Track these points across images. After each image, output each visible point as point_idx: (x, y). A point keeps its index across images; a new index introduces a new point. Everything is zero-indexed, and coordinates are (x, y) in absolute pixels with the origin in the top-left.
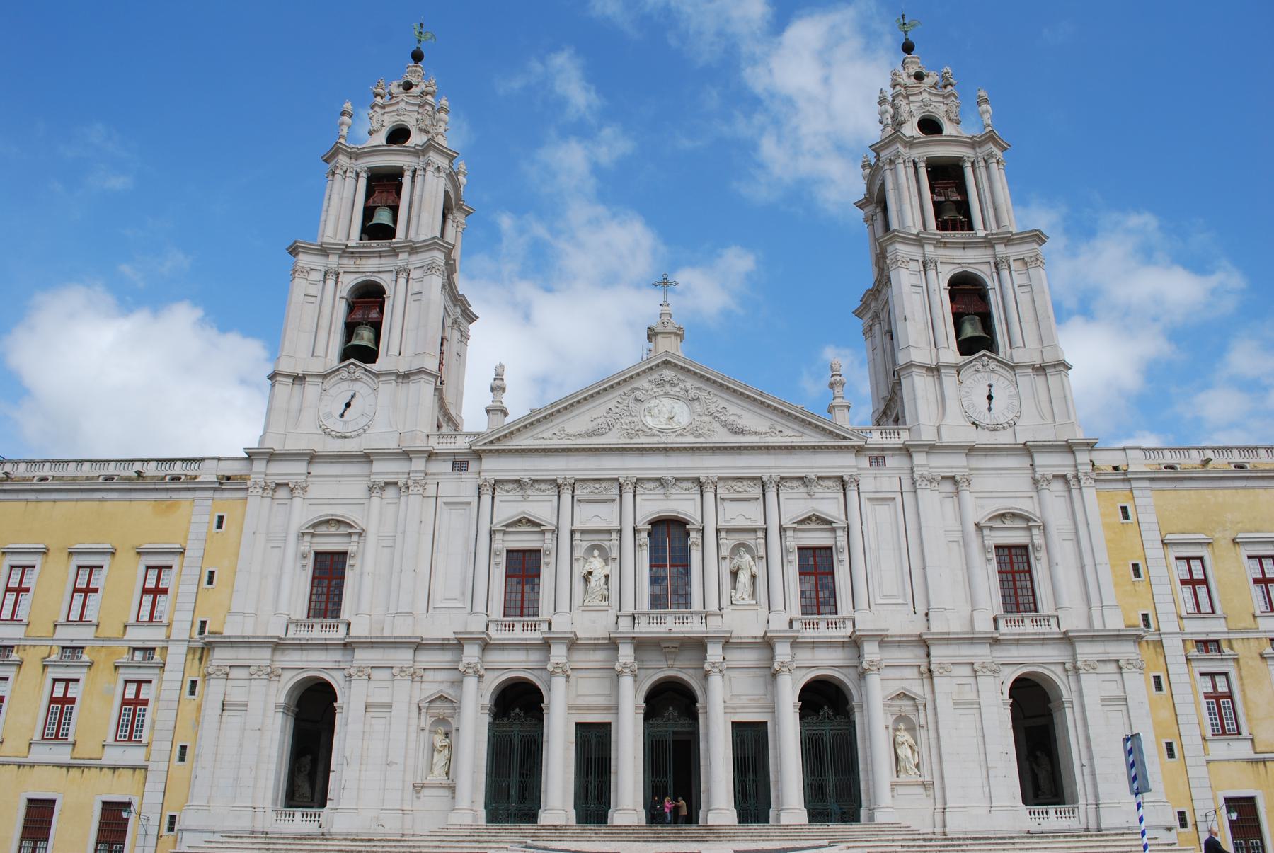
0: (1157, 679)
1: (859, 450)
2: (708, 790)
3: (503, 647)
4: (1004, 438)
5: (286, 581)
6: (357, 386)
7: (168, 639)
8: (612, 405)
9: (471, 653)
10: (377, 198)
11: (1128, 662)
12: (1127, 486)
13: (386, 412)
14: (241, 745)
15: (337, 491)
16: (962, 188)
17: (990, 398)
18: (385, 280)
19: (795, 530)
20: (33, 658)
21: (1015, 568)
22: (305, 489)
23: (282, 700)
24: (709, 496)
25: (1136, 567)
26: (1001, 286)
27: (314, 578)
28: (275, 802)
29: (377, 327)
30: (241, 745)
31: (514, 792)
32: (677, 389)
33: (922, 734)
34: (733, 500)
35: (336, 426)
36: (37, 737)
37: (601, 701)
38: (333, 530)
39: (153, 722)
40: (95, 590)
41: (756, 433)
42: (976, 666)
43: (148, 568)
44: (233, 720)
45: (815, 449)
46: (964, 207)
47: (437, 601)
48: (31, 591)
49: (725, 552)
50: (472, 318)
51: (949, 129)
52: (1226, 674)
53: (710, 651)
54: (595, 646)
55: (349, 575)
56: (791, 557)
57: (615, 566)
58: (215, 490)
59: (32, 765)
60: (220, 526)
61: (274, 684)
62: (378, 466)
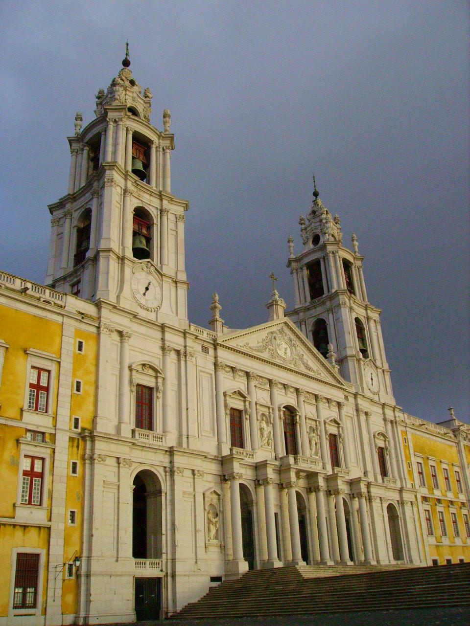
17: (372, 379)
18: (154, 212)
35: (142, 301)
57: (272, 427)
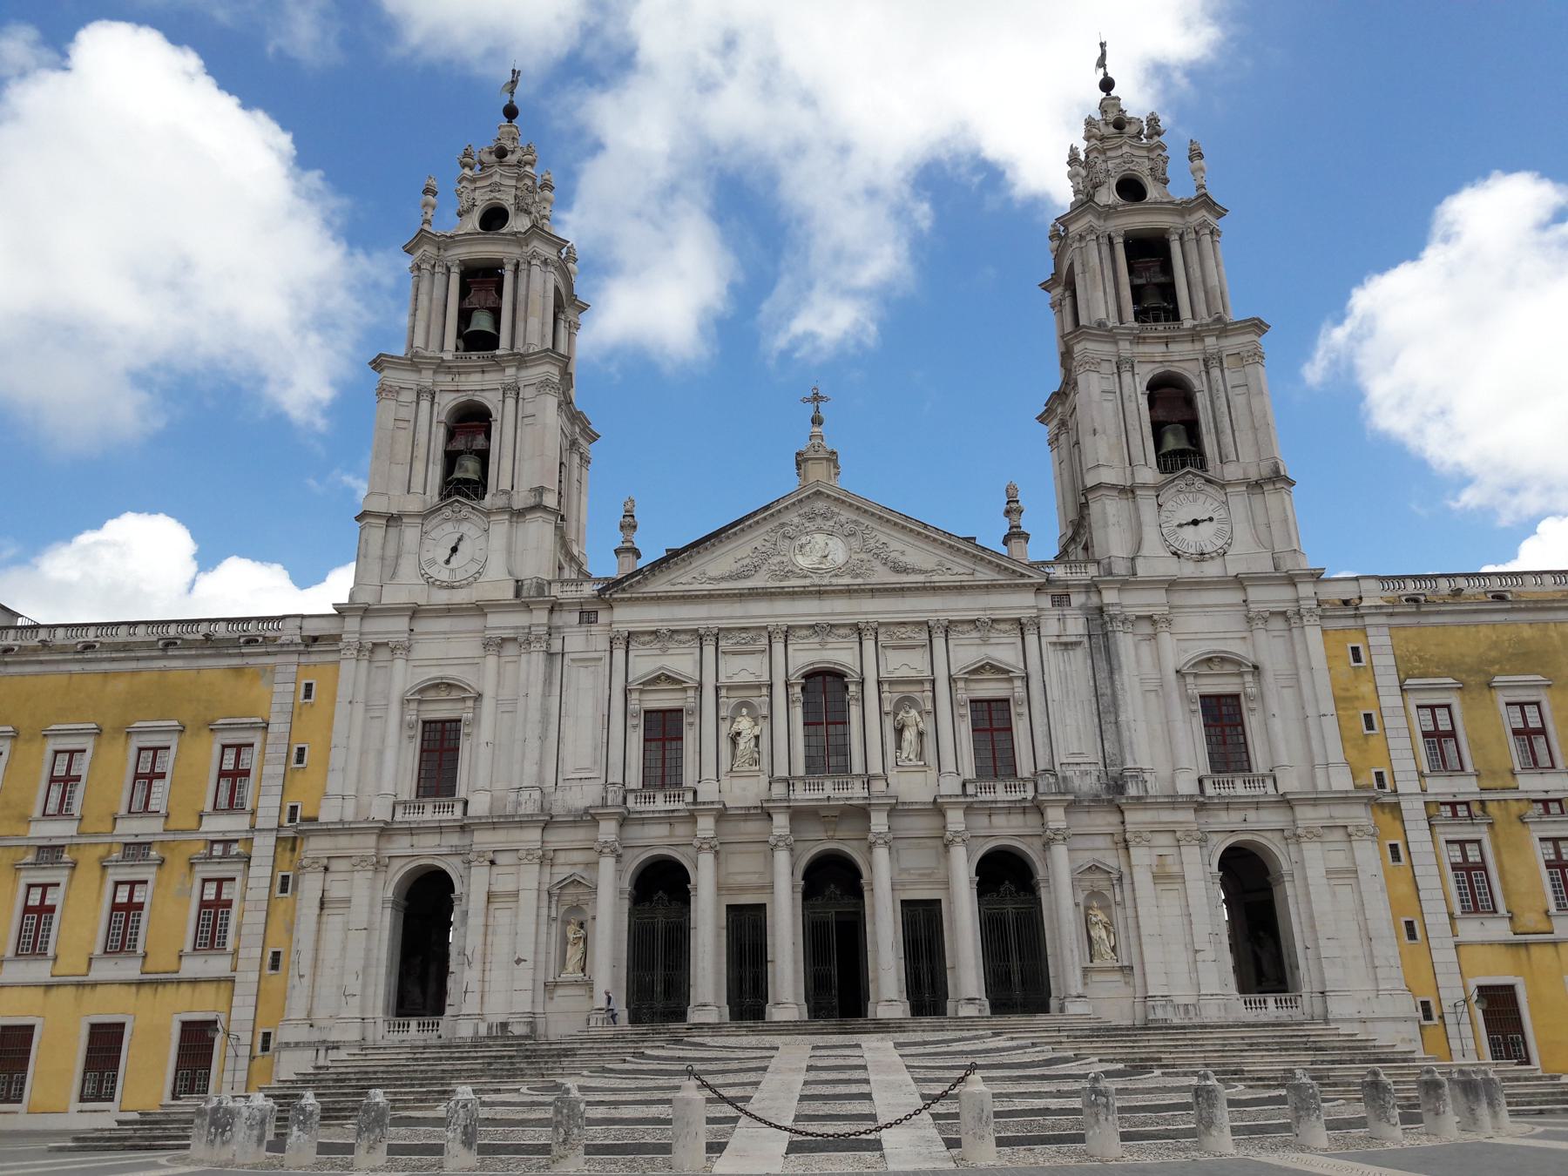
0: (1394, 847)
1: (1039, 589)
2: (877, 979)
3: (643, 821)
4: (1211, 569)
5: (390, 755)
6: (464, 527)
7: (252, 827)
8: (758, 543)
9: (608, 830)
10: (474, 299)
12: (1359, 622)
13: (496, 554)
14: (344, 949)
15: (446, 651)
16: (1167, 268)
18: (491, 401)
19: (966, 680)
20: (89, 858)
21: (1223, 720)
22: (408, 649)
23: (390, 894)
24: (869, 645)
25: (1368, 717)
26: (1210, 388)
27: (422, 751)
28: (386, 1012)
29: (483, 457)
30: (344, 949)
31: (659, 988)
32: (831, 523)
33: (1118, 914)
34: (894, 648)
35: (444, 575)
36: (98, 951)
37: (754, 879)
38: (443, 695)
39: (239, 926)
40: (162, 776)
41: (921, 572)
43: (224, 747)
44: (334, 921)
45: (989, 588)
46: (1168, 291)
47: (568, 770)
48: (83, 780)
49: (887, 708)
50: (593, 437)
51: (1153, 192)
52: (1478, 842)
53: (873, 821)
54: (747, 814)
55: (465, 747)
56: (963, 711)
57: (765, 725)
58: (300, 653)
59: (94, 985)
60: (308, 695)
61: (382, 876)
62: (494, 620)
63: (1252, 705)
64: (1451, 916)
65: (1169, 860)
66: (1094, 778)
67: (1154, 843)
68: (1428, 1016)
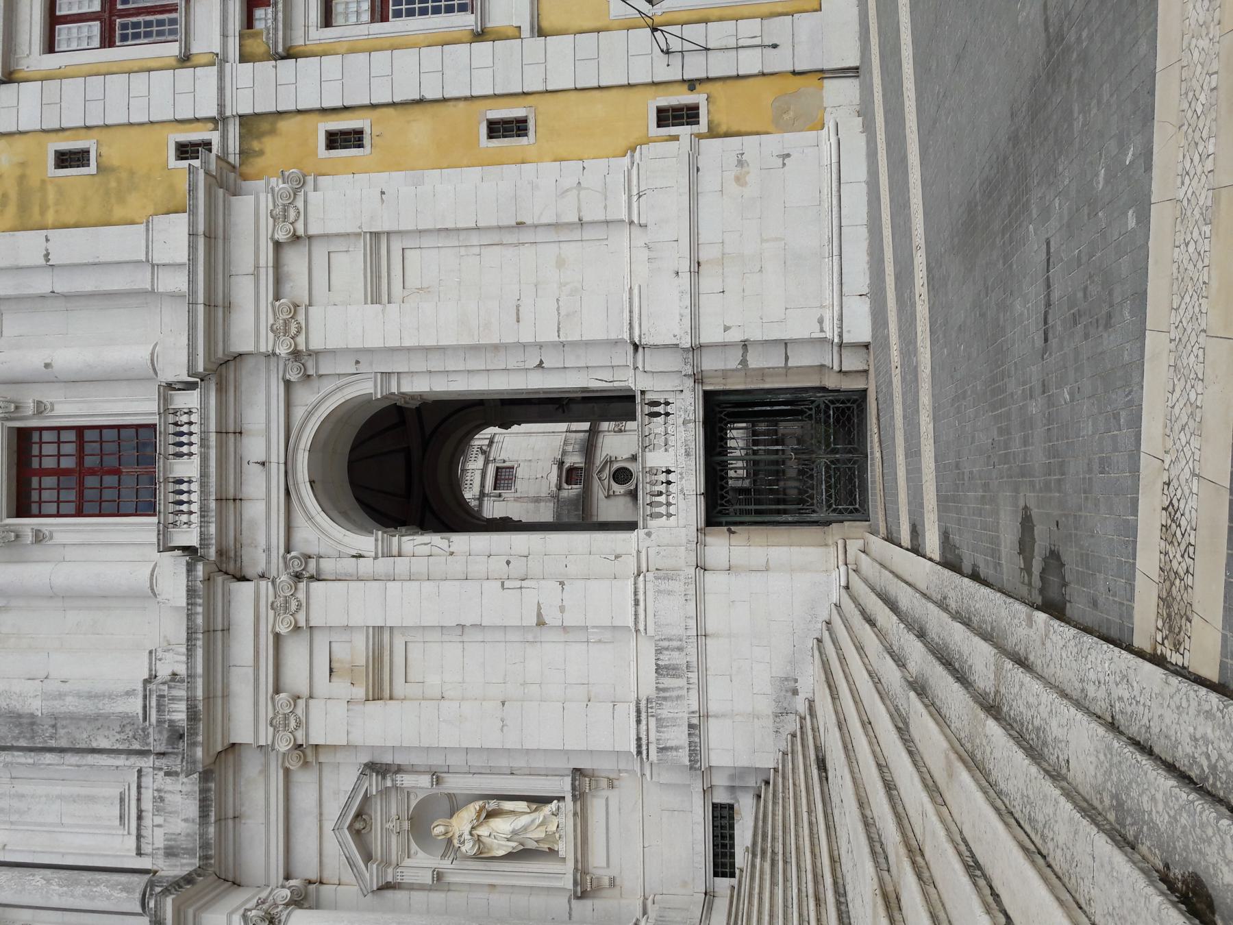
0: (335, 140)
11: (280, 216)
25: (66, 159)
42: (283, 629)
63: (30, 409)
64: (480, 35)
65: (341, 652)
66: (169, 784)
67: (305, 691)
68: (687, 115)
